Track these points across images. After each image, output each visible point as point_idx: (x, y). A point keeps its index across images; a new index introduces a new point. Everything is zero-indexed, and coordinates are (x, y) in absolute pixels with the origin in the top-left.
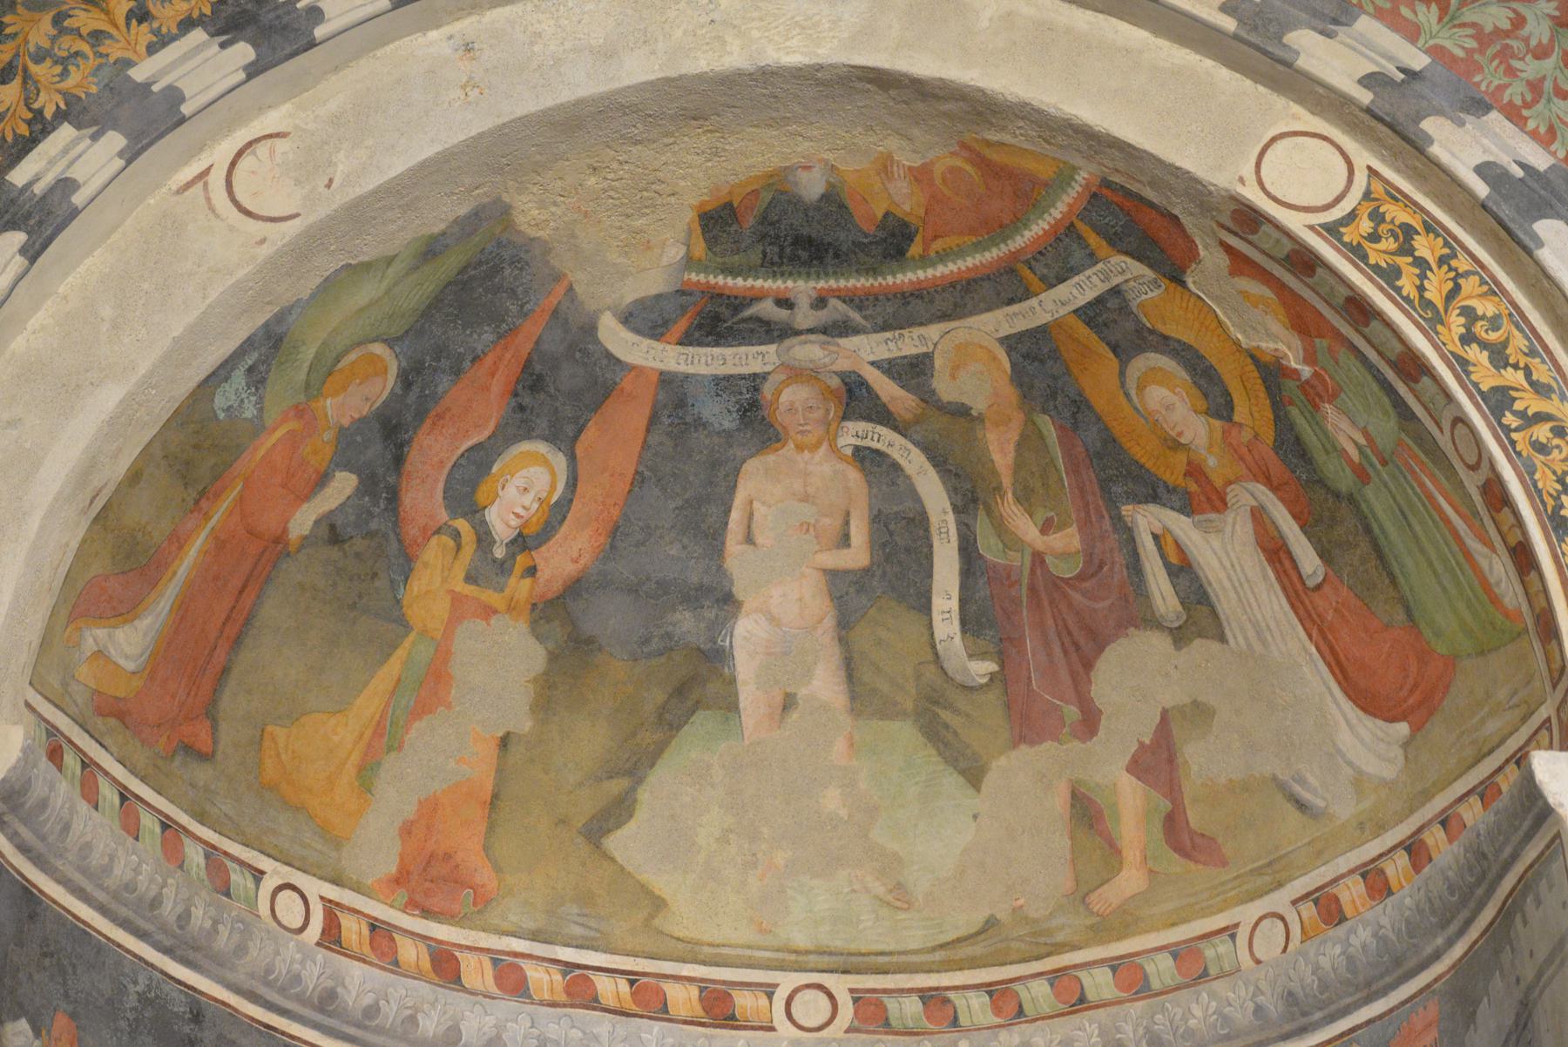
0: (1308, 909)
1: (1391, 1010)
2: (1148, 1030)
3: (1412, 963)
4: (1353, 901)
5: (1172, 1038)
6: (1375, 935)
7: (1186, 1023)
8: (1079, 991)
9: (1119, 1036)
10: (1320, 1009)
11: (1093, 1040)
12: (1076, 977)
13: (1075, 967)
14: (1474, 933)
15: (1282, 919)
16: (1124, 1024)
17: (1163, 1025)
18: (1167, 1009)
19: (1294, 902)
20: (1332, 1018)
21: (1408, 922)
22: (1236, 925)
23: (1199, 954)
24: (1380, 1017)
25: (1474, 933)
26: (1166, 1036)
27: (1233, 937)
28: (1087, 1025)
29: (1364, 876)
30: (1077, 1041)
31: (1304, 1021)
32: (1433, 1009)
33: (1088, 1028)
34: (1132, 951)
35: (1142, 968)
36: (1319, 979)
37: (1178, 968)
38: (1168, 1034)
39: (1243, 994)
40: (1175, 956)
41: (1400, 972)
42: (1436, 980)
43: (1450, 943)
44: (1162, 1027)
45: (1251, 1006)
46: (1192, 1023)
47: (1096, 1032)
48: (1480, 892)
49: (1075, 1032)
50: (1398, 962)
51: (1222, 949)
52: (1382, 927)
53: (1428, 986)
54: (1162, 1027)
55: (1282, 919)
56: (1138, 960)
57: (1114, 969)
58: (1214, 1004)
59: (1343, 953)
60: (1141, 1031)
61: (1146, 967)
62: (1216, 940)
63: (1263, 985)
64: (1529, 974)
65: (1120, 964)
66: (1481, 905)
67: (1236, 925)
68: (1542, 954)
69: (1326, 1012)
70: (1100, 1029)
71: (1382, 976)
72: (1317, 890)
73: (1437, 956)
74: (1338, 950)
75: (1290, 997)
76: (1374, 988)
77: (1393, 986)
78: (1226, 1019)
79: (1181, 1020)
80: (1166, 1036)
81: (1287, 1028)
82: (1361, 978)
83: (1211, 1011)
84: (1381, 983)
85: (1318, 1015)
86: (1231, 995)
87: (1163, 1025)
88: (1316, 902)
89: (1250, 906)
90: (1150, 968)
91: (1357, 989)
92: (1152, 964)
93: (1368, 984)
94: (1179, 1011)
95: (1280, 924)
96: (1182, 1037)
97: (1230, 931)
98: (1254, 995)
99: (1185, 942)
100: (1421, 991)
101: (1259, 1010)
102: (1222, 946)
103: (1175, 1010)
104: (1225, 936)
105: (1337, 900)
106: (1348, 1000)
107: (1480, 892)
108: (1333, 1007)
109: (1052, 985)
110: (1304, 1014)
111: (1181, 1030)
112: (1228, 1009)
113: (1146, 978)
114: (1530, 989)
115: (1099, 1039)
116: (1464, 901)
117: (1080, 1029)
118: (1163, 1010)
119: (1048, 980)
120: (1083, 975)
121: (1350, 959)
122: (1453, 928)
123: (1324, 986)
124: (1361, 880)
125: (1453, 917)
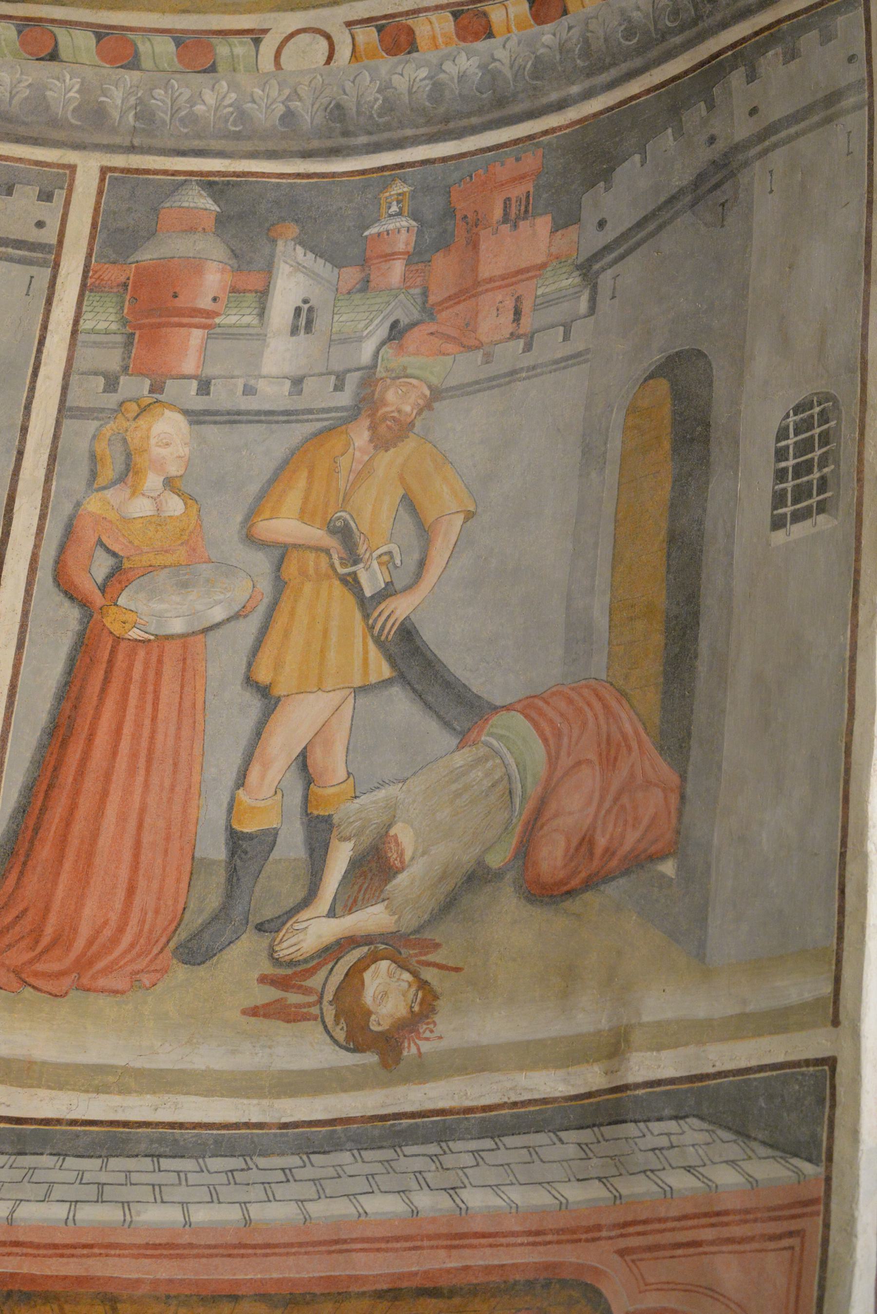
0: (367, 36)
1: (463, 155)
2: (140, 101)
3: (517, 109)
4: (434, 38)
5: (168, 119)
6: (483, 67)
7: (191, 107)
8: (53, 44)
9: (103, 99)
10: (370, 133)
11: (71, 94)
12: (52, 32)
13: (53, 21)
14: (634, 87)
15: (328, 37)
16: (113, 88)
17: (163, 101)
18: (173, 87)
19: (349, 24)
20: (376, 148)
21: (538, 59)
22: (265, 31)
23: (211, 48)
24: (444, 160)
25: (634, 87)
26: (162, 115)
27: (257, 42)
28: (68, 77)
29: (455, 15)
30: (50, 89)
31: (343, 141)
32: (531, 161)
33: (67, 80)
34: (126, 24)
35: (134, 45)
36: (385, 100)
37: (179, 56)
38: (166, 114)
39: (274, 93)
40: (178, 42)
41: (496, 115)
42: (545, 133)
43: (588, 95)
44: (160, 104)
45: (280, 109)
46: (199, 108)
47: (77, 87)
48: (678, 40)
49: (51, 80)
50: (500, 102)
51: (239, 50)
52: (494, 60)
53: (530, 137)
54: (160, 104)
55: (328, 37)
56: (130, 35)
57: (99, 37)
58: (233, 96)
59: (430, 77)
60: (132, 100)
61: (140, 45)
62: (235, 40)
63: (303, 90)
64: (743, 130)
65: (108, 34)
66: (669, 55)
67: (265, 31)
68: (776, 112)
69: (374, 138)
70: (82, 84)
71: (469, 115)
72: (385, 17)
73: (561, 106)
74: (423, 73)
75: (337, 112)
76: (452, 125)
77: (474, 130)
78: (242, 116)
79: (187, 101)
80: (162, 115)
81: (315, 144)
82: (442, 110)
83: (227, 102)
84: (464, 122)
85: (363, 139)
86: (258, 91)
87: (163, 101)
88: (380, 29)
89: (289, 15)
90: (144, 48)
91: (428, 123)
92: (148, 44)
93: (447, 121)
94: (187, 94)
95: (324, 44)
96: (182, 120)
97: (256, 36)
98: (288, 98)
99: (194, 32)
100: (516, 142)
101: (289, 116)
102: (241, 48)
103: (182, 90)
104: (247, 39)
105: (411, 32)
106: (409, 132)
107: (678, 40)
108: (386, 135)
109: (19, 32)
110: (346, 134)
111: (183, 113)
112: (250, 105)
113: (136, 55)
114: (737, 148)
115: (78, 96)
116: (642, 49)
117: (58, 79)
118: (167, 86)
119: (17, 26)
120: (61, 34)
121: (438, 88)
122: (604, 78)
123: (389, 107)
124: (451, 18)
125: (613, 64)
